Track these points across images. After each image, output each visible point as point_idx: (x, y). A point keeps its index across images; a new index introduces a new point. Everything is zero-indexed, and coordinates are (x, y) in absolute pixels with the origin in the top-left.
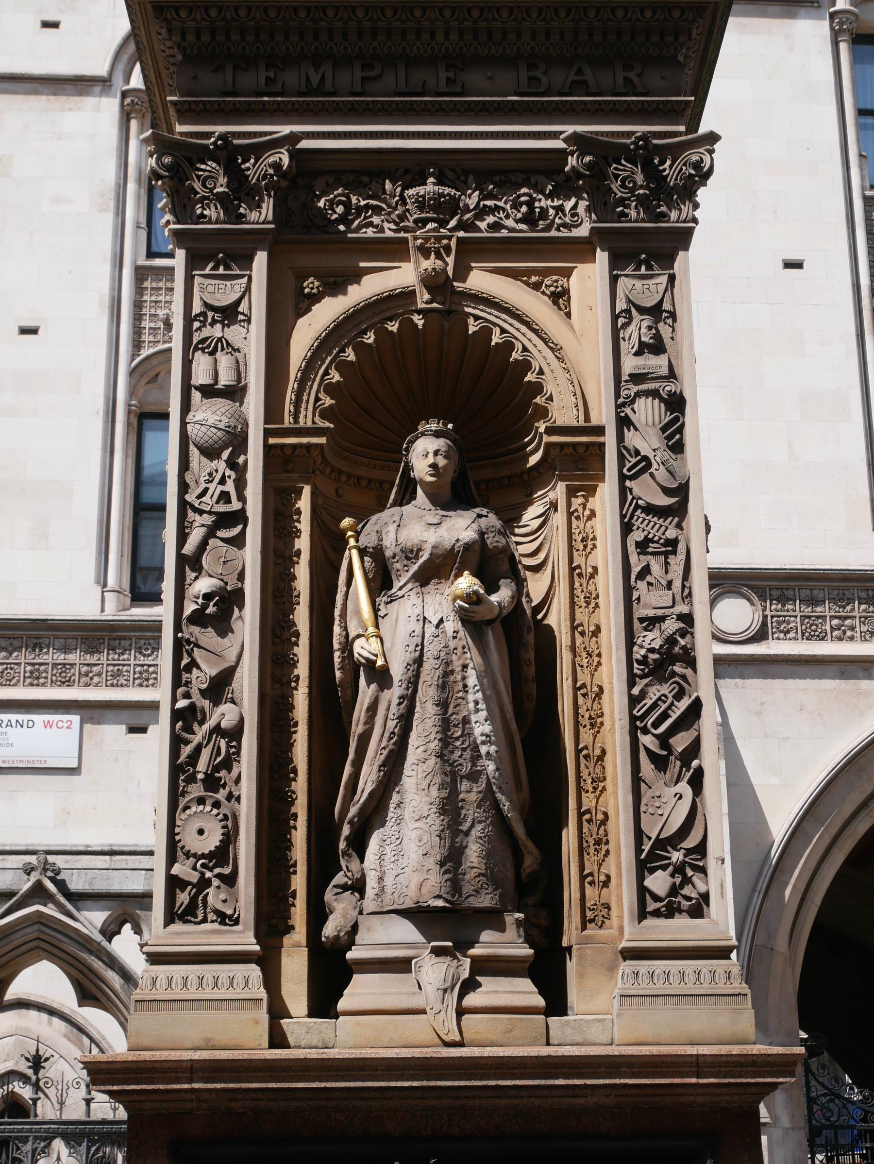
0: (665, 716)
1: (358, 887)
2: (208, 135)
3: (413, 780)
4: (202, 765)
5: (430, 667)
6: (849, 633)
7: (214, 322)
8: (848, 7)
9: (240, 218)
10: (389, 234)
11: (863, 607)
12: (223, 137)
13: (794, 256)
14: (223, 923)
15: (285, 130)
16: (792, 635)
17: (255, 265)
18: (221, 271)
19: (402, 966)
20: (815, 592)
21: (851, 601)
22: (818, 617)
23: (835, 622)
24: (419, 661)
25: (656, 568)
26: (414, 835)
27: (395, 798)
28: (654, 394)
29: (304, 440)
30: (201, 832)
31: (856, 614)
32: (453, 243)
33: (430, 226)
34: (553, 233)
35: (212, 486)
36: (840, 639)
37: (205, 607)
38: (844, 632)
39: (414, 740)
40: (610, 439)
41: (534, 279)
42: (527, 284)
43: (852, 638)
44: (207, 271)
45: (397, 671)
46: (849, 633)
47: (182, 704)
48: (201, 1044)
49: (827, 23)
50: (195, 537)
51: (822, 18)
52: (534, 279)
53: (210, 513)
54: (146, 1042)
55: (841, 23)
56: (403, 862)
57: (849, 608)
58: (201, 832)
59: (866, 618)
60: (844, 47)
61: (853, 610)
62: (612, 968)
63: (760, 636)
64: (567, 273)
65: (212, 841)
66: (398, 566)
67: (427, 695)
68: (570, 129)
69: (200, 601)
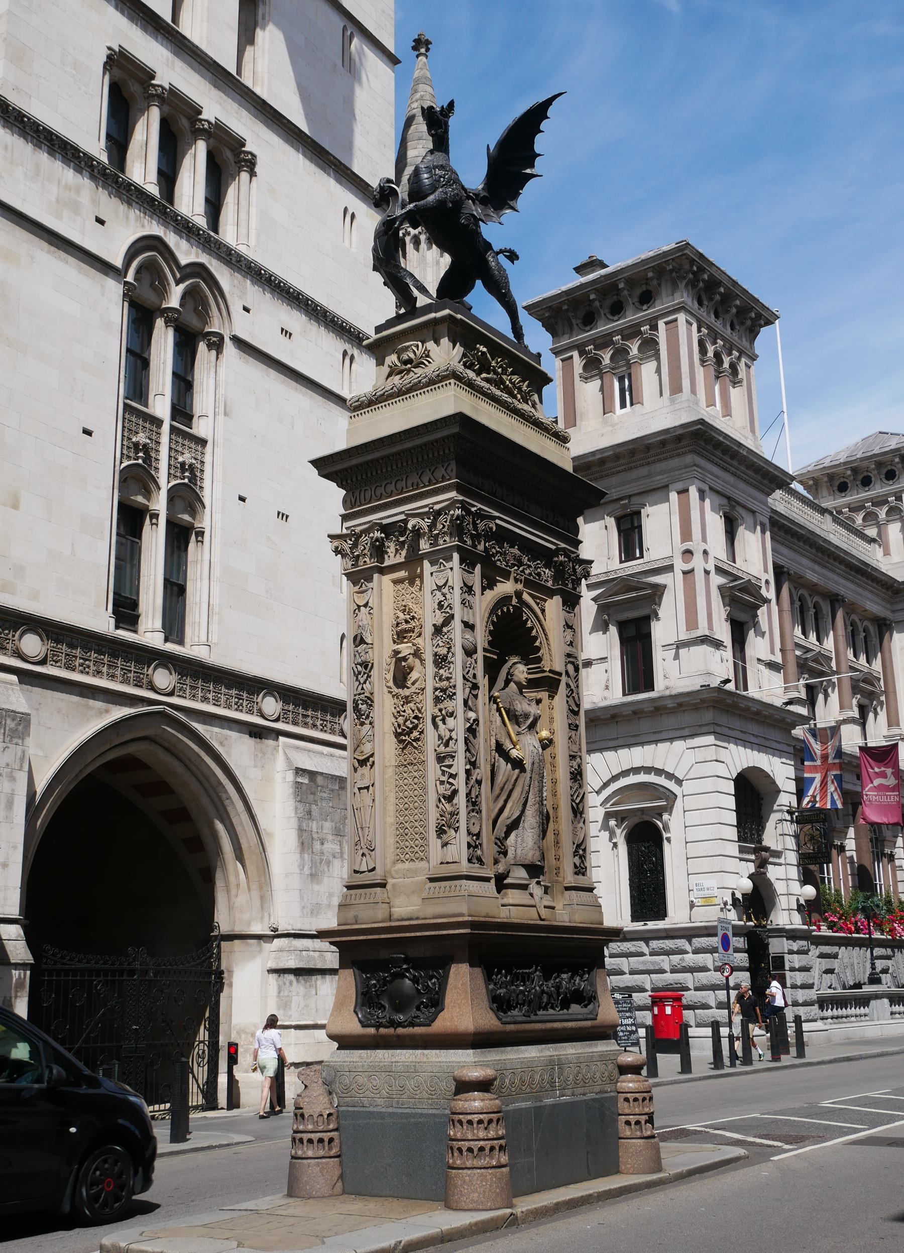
0: (578, 796)
1: (505, 853)
2: (474, 506)
3: (531, 812)
4: (473, 795)
5: (536, 765)
6: (87, 670)
7: (466, 592)
8: (132, 281)
9: (475, 546)
10: (503, 566)
11: (96, 655)
12: (480, 509)
13: (89, 428)
14: (481, 864)
15: (497, 514)
16: (58, 664)
17: (476, 569)
18: (466, 568)
19: (524, 887)
20: (74, 640)
21: (90, 650)
22: (73, 656)
23: (81, 661)
24: (533, 763)
25: (573, 735)
26: (530, 834)
27: (523, 818)
28: (573, 663)
29: (492, 656)
30: (474, 824)
31: (91, 658)
32: (523, 578)
33: (516, 568)
34: (543, 583)
35: (471, 670)
36: (82, 672)
37: (472, 725)
38: (85, 669)
39: (531, 796)
40: (564, 679)
41: (538, 601)
42: (536, 602)
43: (88, 673)
44: (463, 567)
45: (528, 766)
46: (87, 670)
47: (468, 767)
48: (485, 914)
49: (122, 286)
50: (468, 690)
51: (120, 283)
52: (538, 601)
53: (471, 682)
54: (472, 913)
55: (128, 290)
56: (525, 845)
57: (88, 654)
58: (474, 824)
59: (96, 662)
60: (126, 304)
61: (90, 656)
62: (563, 893)
63: (43, 662)
64: (545, 601)
65: (475, 830)
66: (521, 720)
67: (536, 777)
68: (563, 545)
69: (471, 721)
